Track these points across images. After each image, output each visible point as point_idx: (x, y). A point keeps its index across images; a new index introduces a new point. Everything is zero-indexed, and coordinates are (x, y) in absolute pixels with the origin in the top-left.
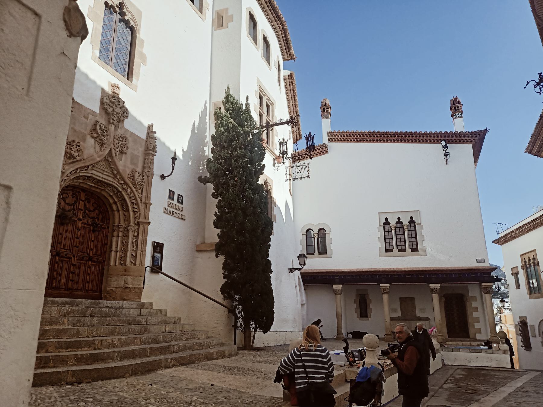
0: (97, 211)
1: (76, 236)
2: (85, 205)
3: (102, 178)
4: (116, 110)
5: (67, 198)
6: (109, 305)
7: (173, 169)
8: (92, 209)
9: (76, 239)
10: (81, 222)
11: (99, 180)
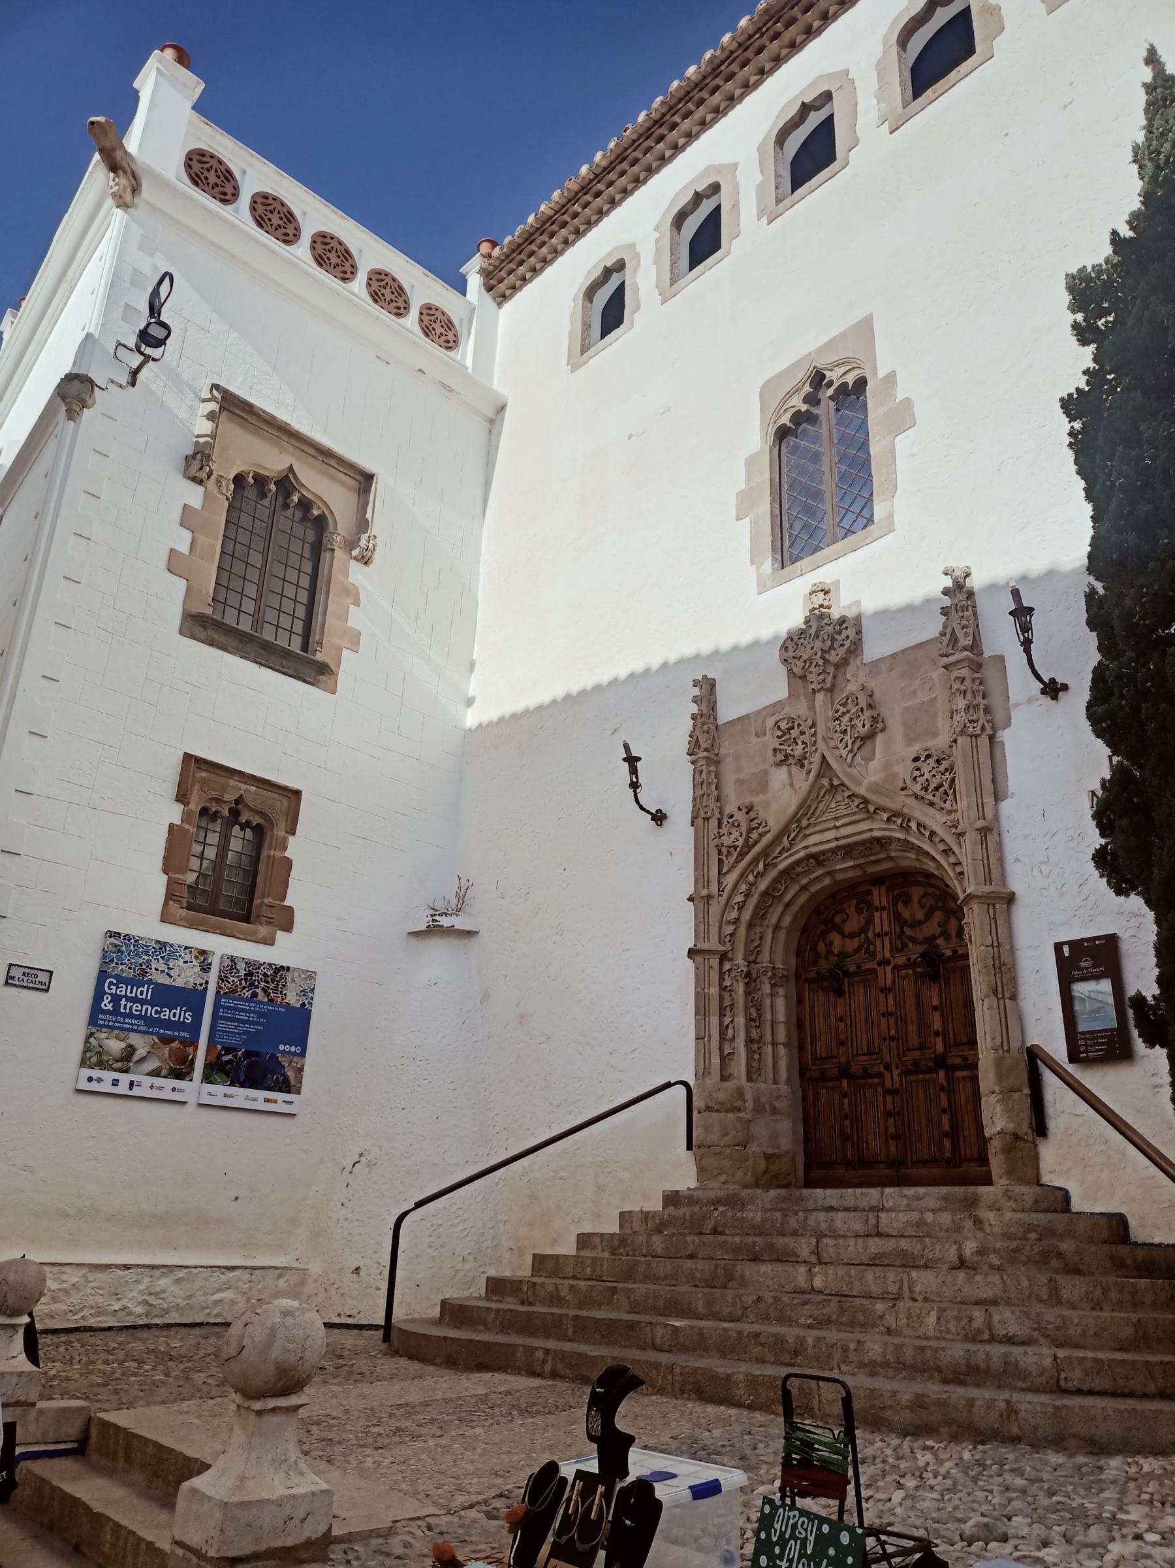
0: (938, 916)
1: (883, 1010)
2: (897, 917)
3: (837, 839)
5: (845, 921)
6: (834, 1203)
7: (1028, 651)
8: (920, 915)
9: (884, 1021)
10: (889, 969)
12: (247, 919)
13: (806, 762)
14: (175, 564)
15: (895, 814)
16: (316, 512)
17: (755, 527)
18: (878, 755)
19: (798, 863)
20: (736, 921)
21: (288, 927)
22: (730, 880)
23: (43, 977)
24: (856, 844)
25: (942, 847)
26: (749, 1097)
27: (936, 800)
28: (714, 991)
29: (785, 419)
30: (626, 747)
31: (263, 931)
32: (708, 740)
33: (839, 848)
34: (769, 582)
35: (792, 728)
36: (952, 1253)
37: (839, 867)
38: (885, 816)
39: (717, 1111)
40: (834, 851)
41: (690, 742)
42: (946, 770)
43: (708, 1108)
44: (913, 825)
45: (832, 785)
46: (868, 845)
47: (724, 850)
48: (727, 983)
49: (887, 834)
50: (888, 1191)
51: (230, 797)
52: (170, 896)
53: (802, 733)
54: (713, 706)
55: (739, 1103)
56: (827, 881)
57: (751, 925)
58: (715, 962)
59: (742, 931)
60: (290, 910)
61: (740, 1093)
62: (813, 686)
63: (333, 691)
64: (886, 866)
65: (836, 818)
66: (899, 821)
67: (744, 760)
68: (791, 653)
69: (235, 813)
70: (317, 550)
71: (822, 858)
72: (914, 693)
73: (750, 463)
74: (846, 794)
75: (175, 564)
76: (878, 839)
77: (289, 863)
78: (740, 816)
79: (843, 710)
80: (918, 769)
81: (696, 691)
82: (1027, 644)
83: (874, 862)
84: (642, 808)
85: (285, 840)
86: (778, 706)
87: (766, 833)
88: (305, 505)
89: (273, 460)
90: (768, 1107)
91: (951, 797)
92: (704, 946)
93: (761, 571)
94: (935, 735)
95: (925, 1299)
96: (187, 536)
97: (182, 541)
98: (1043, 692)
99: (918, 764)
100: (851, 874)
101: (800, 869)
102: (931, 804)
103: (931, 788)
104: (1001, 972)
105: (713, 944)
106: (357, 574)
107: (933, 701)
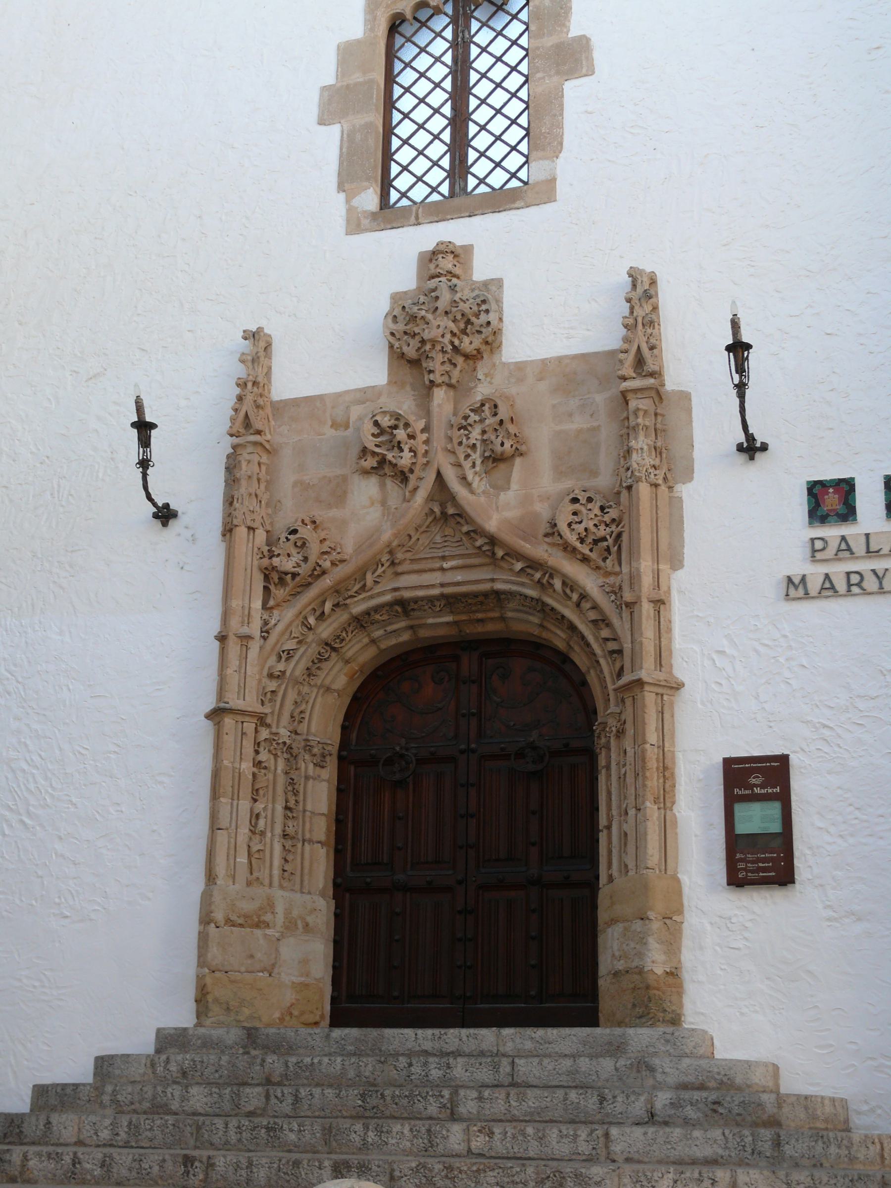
3: (442, 585)
4: (426, 335)
6: (428, 1046)
7: (741, 396)
11: (475, 595)
13: (412, 478)
15: (533, 564)
18: (514, 486)
19: (377, 609)
24: (465, 595)
25: (593, 615)
26: (280, 909)
27: (593, 555)
32: (254, 419)
33: (443, 596)
34: (366, 222)
35: (396, 427)
36: (638, 1107)
37: (430, 621)
38: (519, 566)
39: (241, 925)
40: (431, 600)
41: (233, 420)
42: (614, 520)
43: (229, 922)
44: (557, 584)
45: (444, 513)
46: (481, 598)
47: (275, 577)
48: (264, 756)
49: (514, 588)
50: (507, 1032)
53: (411, 437)
55: (268, 917)
56: (405, 637)
58: (250, 727)
61: (270, 905)
62: (432, 377)
64: (490, 627)
65: (444, 558)
66: (538, 575)
68: (401, 327)
71: (413, 606)
72: (571, 415)
74: (465, 529)
76: (497, 593)
78: (305, 532)
79: (474, 417)
80: (575, 514)
82: (741, 388)
83: (481, 621)
84: (149, 497)
86: (365, 395)
87: (342, 561)
90: (300, 925)
91: (614, 556)
92: (239, 704)
93: (355, 202)
94: (594, 473)
95: (628, 1160)
98: (740, 448)
99: (577, 506)
100: (441, 632)
101: (378, 617)
102: (585, 560)
103: (589, 540)
104: (664, 776)
105: (250, 702)
107: (595, 430)
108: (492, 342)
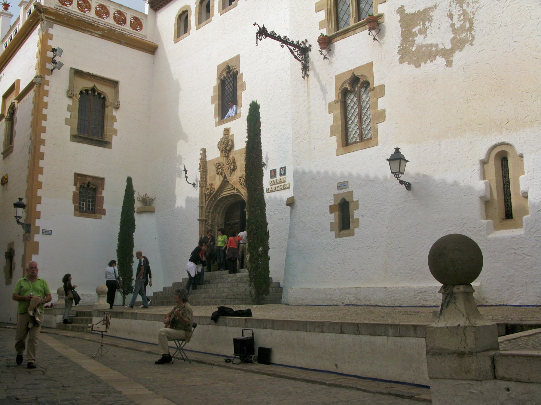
12: (94, 213)
14: (67, 122)
16: (102, 96)
17: (215, 108)
20: (209, 212)
21: (104, 213)
22: (207, 202)
23: (50, 232)
28: (203, 229)
29: (222, 77)
30: (184, 167)
31: (98, 216)
36: (227, 281)
51: (87, 182)
52: (75, 210)
54: (205, 157)
57: (212, 213)
58: (204, 222)
59: (210, 214)
60: (104, 210)
63: (111, 148)
67: (212, 170)
69: (88, 186)
70: (104, 106)
73: (214, 87)
75: (67, 122)
77: (103, 197)
78: (209, 187)
81: (201, 152)
85: (101, 192)
88: (99, 94)
89: (89, 84)
96: (69, 113)
97: (68, 115)
106: (114, 113)
108: (232, 147)
